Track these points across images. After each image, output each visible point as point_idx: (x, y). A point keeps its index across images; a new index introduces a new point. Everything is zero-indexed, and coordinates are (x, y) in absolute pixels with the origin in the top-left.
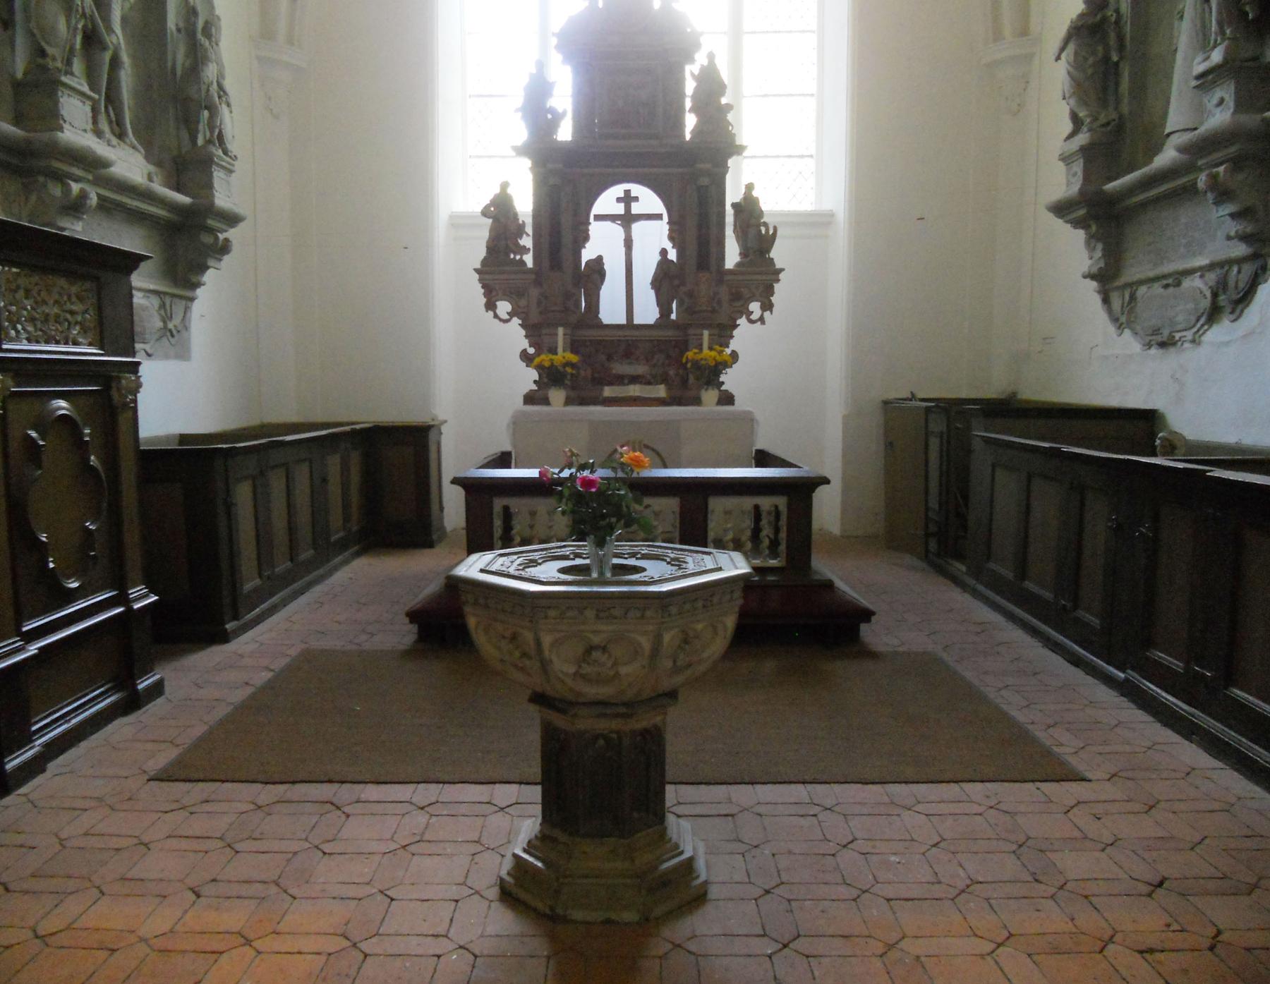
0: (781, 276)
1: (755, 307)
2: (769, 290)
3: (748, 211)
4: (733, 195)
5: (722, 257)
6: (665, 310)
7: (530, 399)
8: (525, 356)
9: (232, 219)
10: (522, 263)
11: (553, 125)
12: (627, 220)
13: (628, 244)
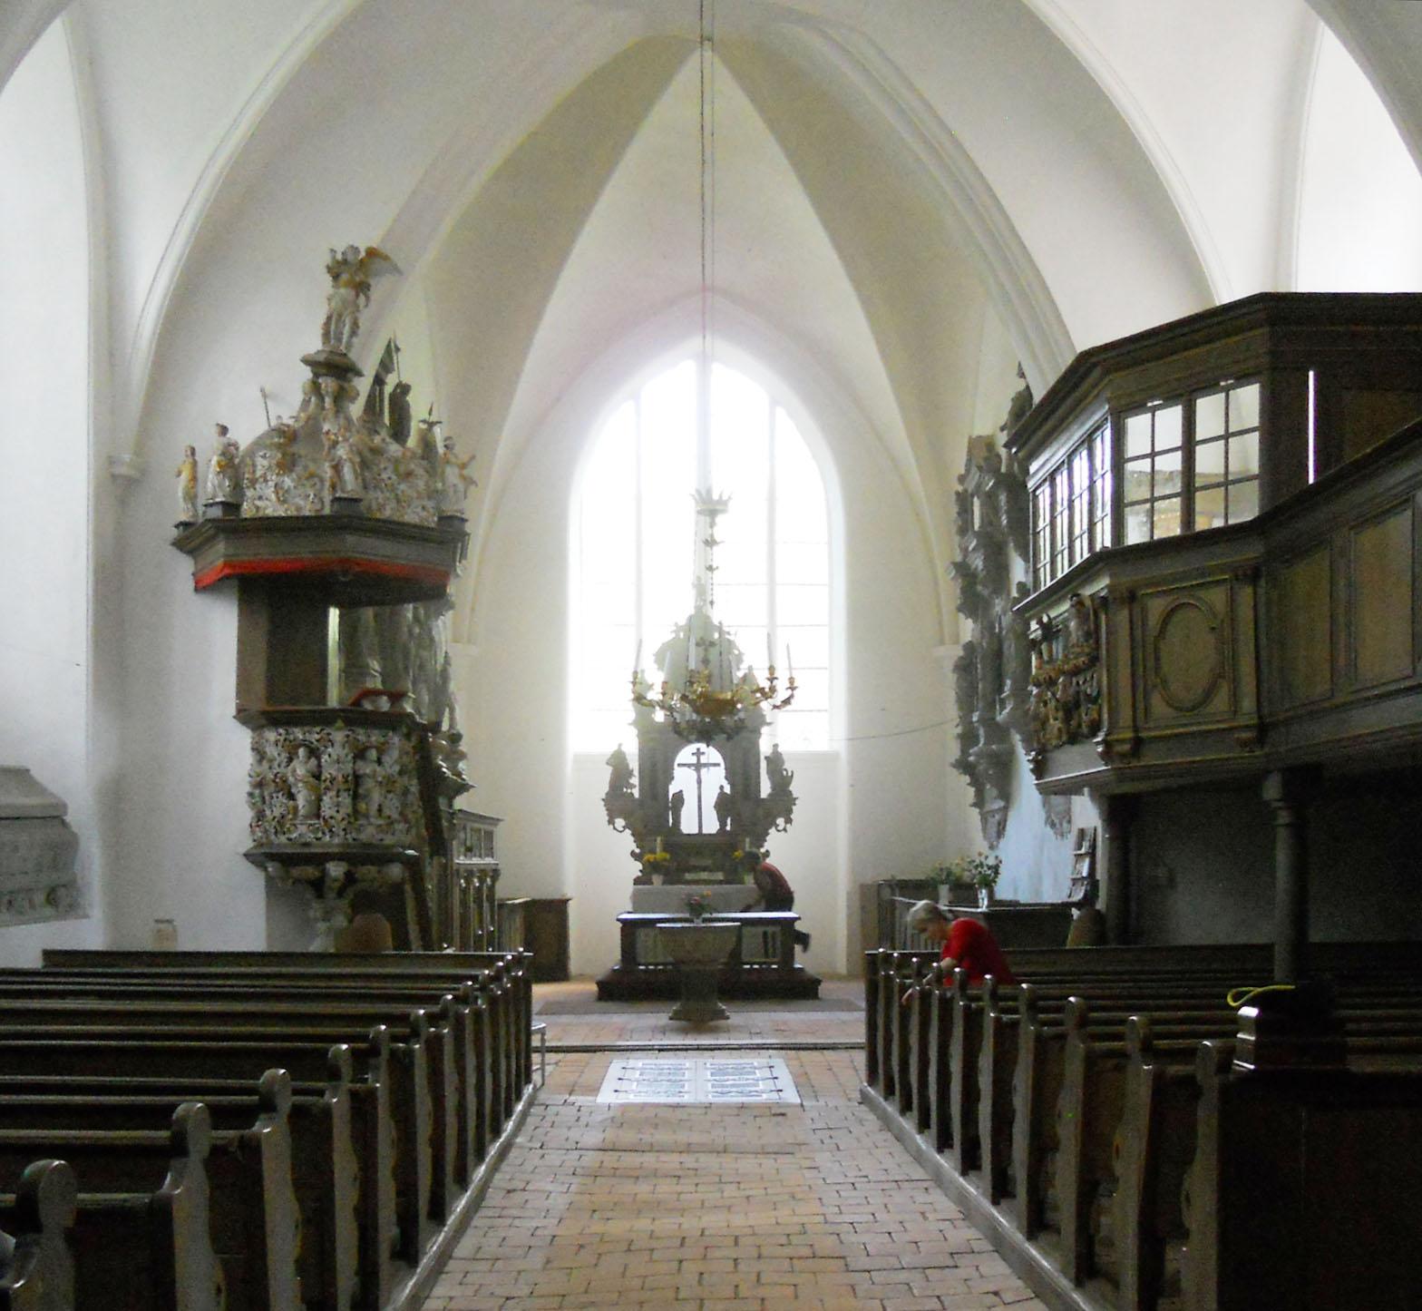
1: (780, 821)
2: (790, 811)
3: (775, 761)
4: (765, 747)
6: (723, 824)
7: (637, 881)
8: (633, 854)
10: (632, 794)
12: (698, 767)
13: (699, 782)
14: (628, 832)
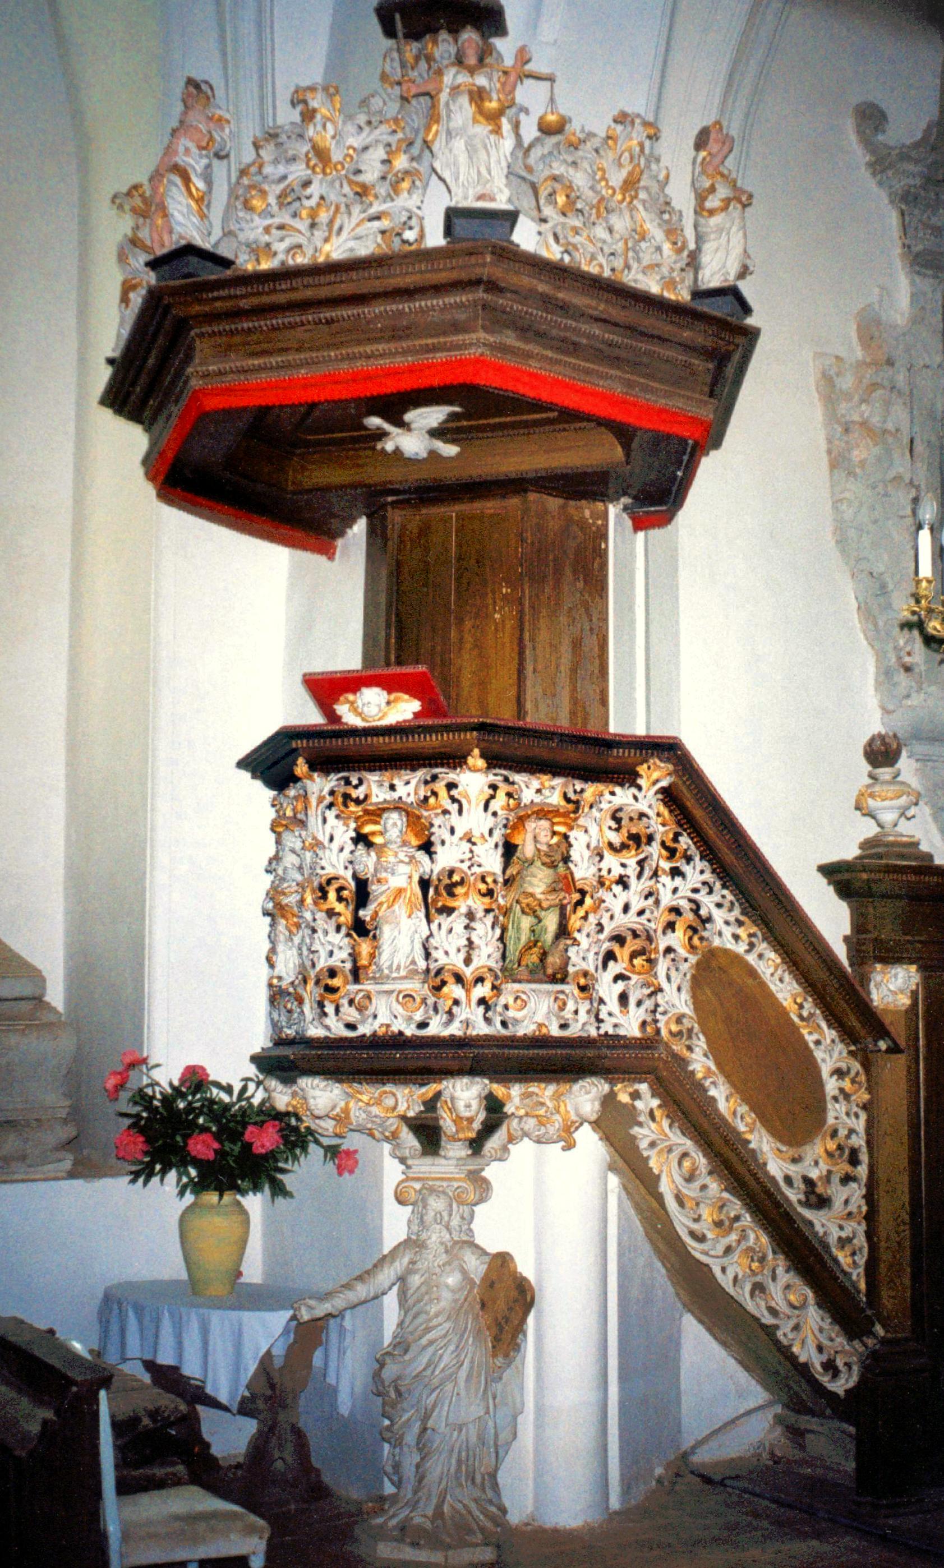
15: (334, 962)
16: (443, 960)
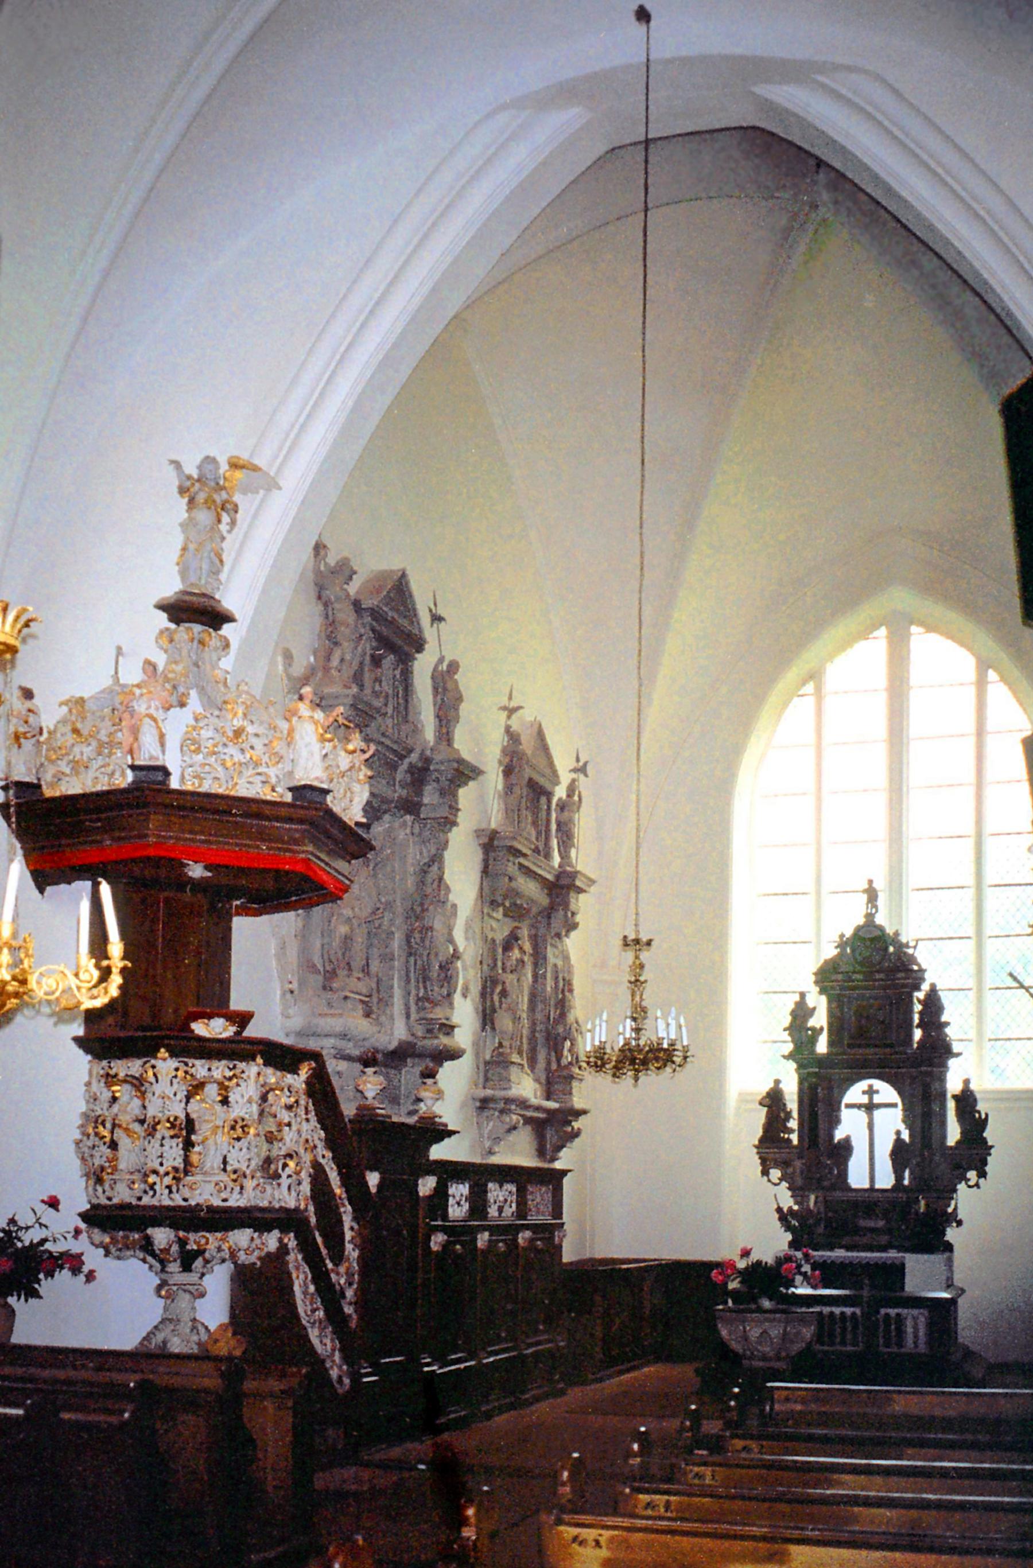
0: (992, 1151)
1: (972, 1175)
3: (966, 1100)
4: (953, 1085)
5: (944, 1137)
6: (899, 1178)
9: (579, 1113)
10: (789, 1141)
11: (813, 1040)
12: (870, 1108)
13: (871, 1126)
14: (785, 1184)
15: (176, 1164)
16: (236, 1166)
